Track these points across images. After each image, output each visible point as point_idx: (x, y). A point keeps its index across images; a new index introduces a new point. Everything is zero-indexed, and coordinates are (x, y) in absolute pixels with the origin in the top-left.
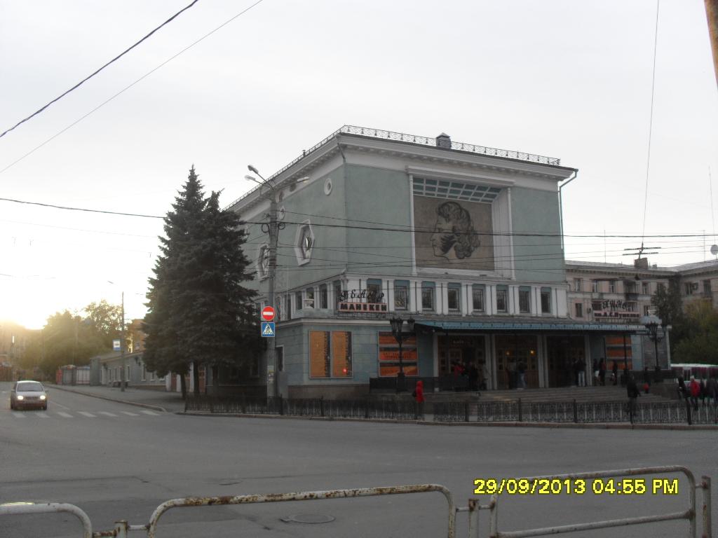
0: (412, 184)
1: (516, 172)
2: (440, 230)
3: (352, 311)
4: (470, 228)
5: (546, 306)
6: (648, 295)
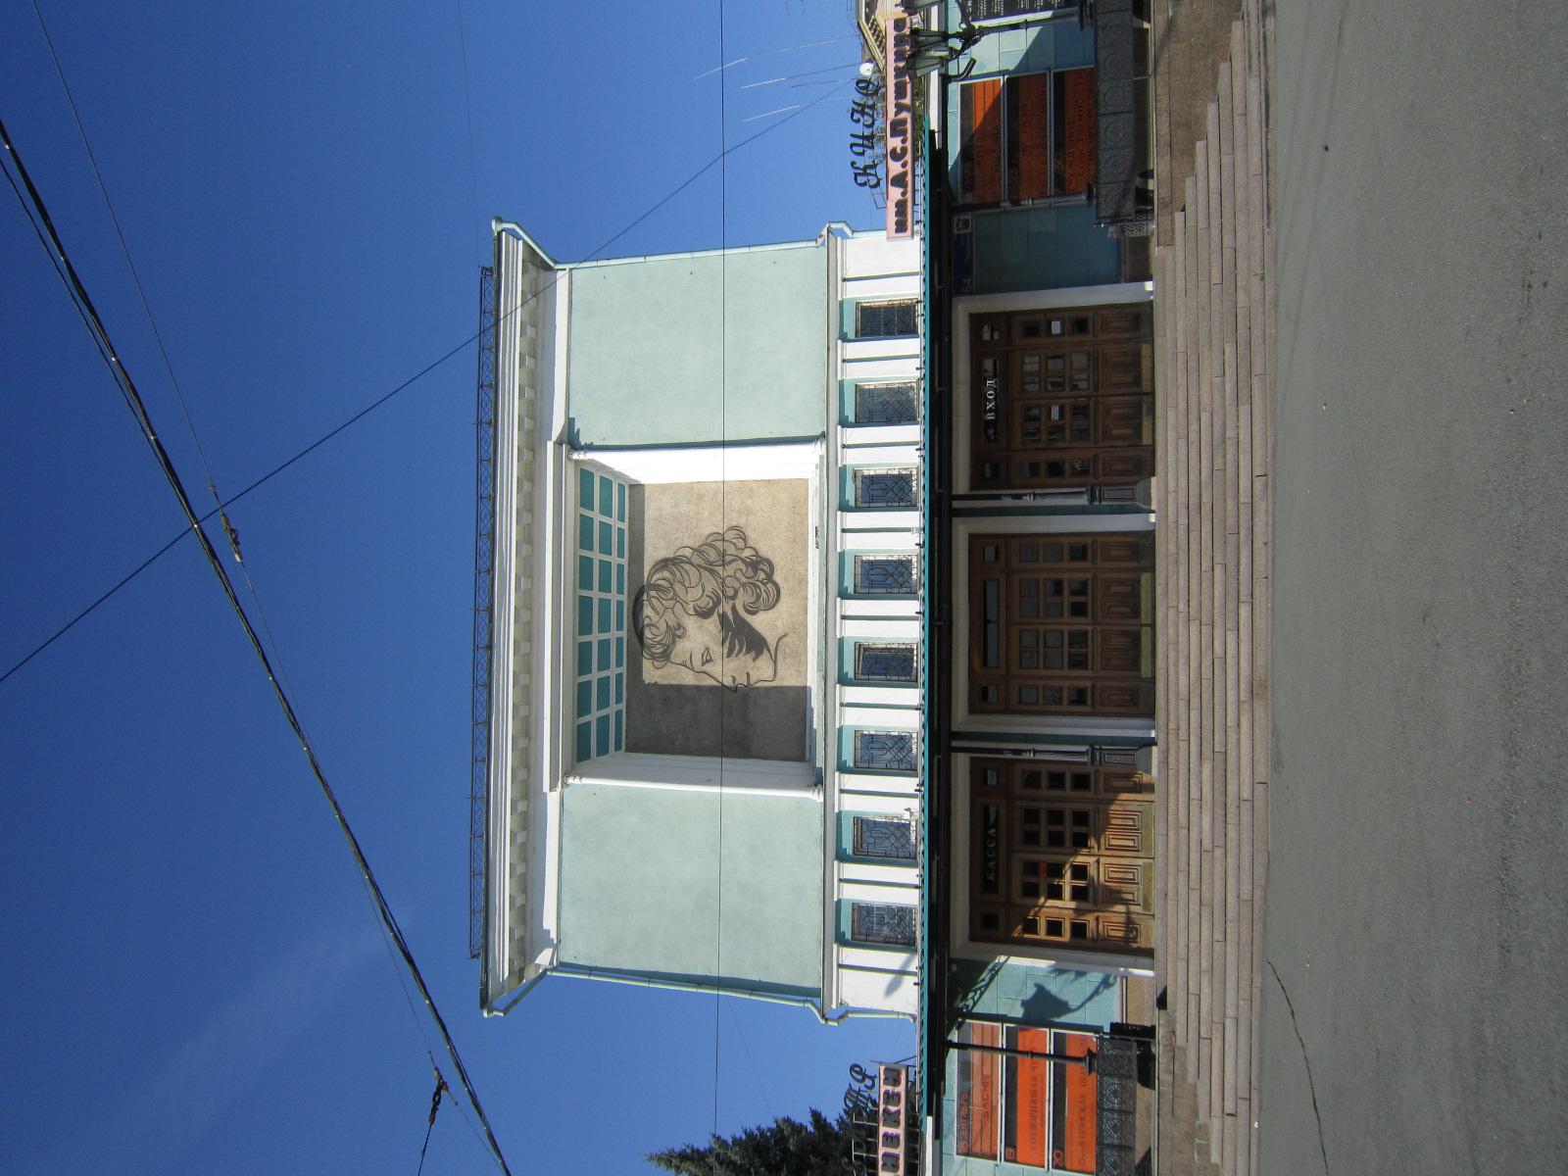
4: (696, 560)
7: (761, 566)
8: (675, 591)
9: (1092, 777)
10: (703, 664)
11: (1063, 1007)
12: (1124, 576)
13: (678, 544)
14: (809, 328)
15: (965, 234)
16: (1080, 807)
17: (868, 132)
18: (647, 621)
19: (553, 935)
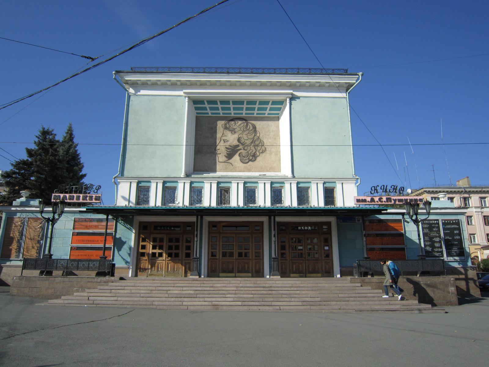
4: (256, 138)
7: (254, 158)
8: (246, 131)
9: (189, 259)
10: (223, 140)
11: (119, 250)
12: (250, 268)
13: (261, 132)
14: (327, 172)
15: (356, 220)
16: (180, 255)
17: (388, 190)
18: (236, 122)
19: (139, 93)
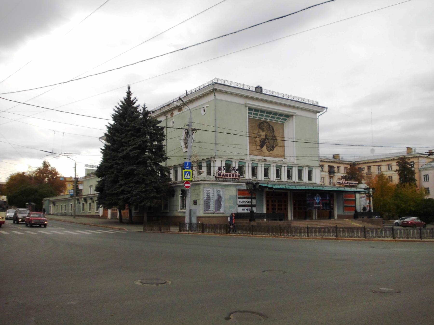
0: (248, 111)
1: (298, 108)
2: (260, 136)
3: (223, 177)
5: (310, 178)
6: (340, 173)
